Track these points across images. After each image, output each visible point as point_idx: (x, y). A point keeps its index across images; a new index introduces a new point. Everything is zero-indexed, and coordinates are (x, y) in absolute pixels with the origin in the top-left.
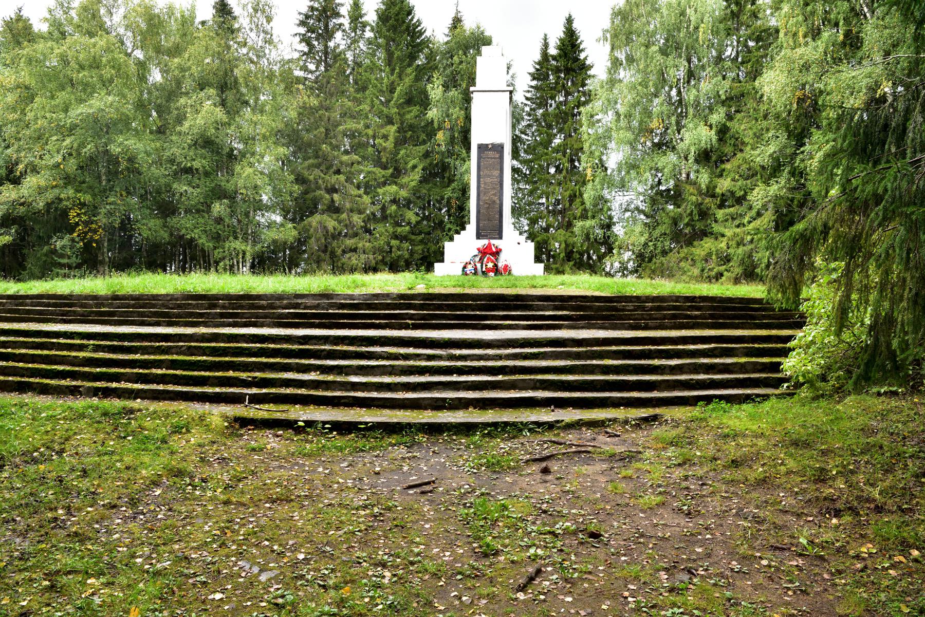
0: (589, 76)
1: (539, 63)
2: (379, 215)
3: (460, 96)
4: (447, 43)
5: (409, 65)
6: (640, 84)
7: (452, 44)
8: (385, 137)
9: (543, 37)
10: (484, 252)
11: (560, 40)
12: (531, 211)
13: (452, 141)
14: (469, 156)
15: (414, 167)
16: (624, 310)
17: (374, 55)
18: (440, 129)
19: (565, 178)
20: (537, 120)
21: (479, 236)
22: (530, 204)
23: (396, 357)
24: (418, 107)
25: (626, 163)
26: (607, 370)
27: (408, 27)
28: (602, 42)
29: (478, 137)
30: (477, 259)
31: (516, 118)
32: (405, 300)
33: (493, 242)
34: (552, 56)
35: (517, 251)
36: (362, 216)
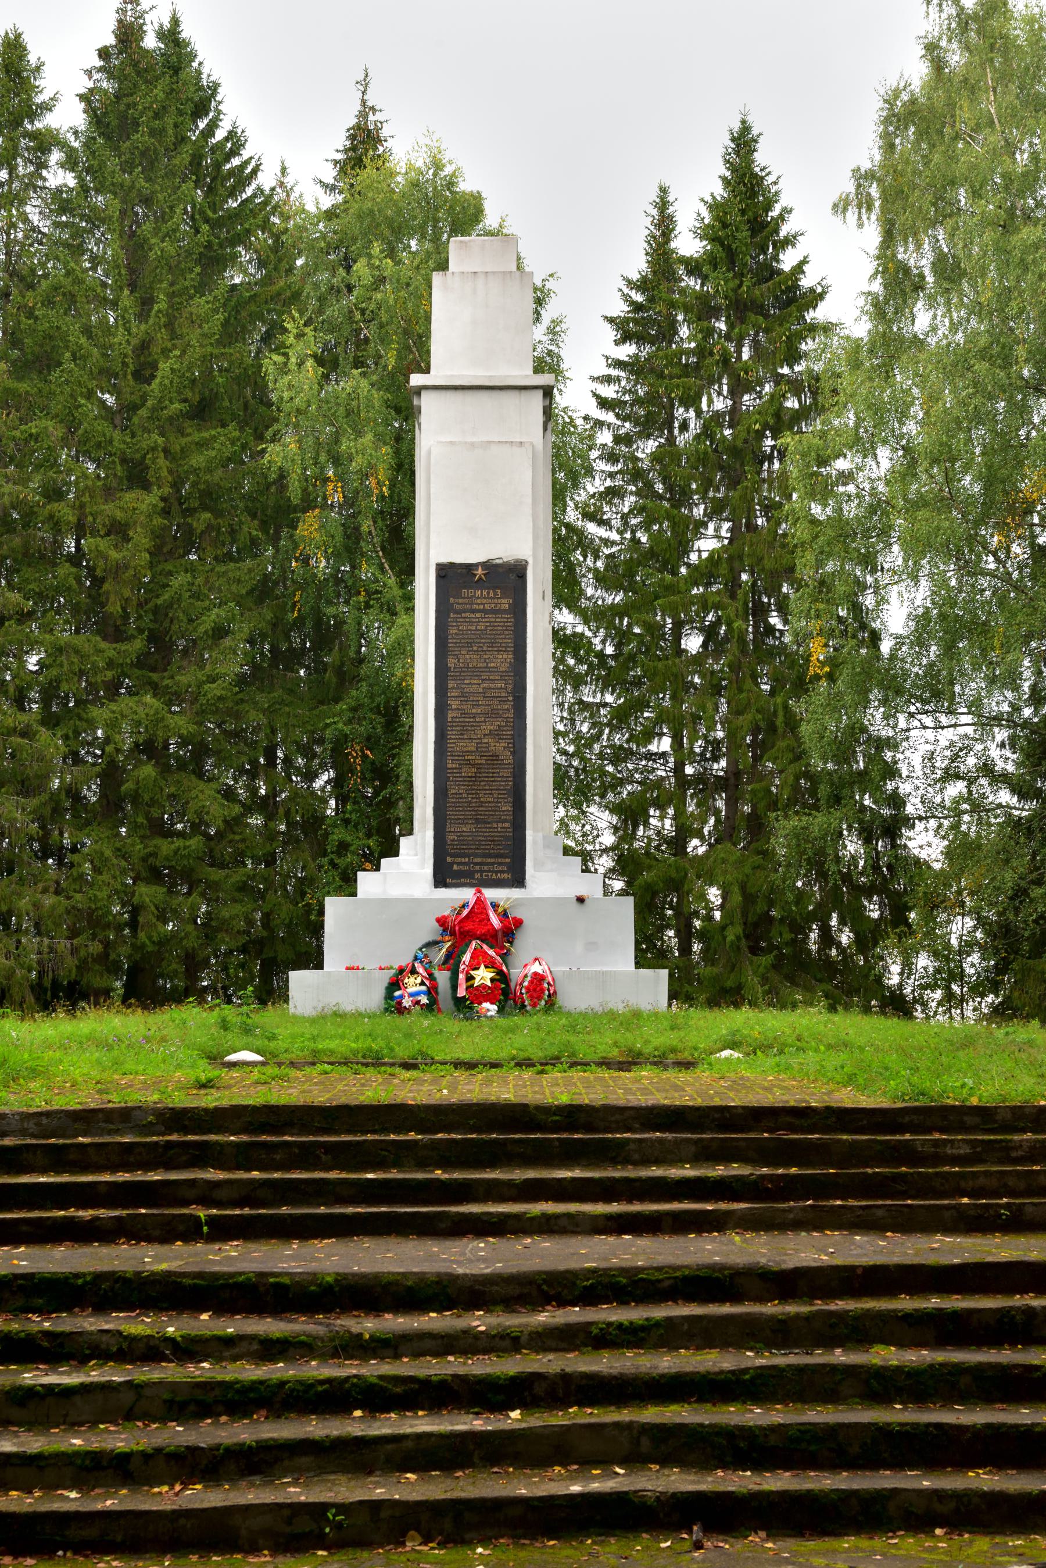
0: (812, 329)
1: (642, 285)
2: (91, 793)
3: (377, 396)
4: (330, 215)
5: (201, 288)
6: (984, 354)
7: (346, 219)
8: (119, 530)
9: (654, 195)
10: (462, 931)
11: (714, 207)
12: (621, 782)
13: (350, 545)
14: (409, 597)
15: (220, 632)
16: (937, 1159)
17: (78, 250)
18: (308, 504)
19: (735, 667)
20: (637, 475)
21: (442, 877)
22: (619, 755)
23: (151, 1351)
24: (233, 430)
25: (943, 617)
26: (881, 1386)
27: (196, 159)
28: (852, 215)
29: (442, 537)
30: (439, 955)
31: (566, 469)
32: (184, 1133)
33: (491, 894)
34: (686, 261)
35: (575, 920)
36: (34, 802)
